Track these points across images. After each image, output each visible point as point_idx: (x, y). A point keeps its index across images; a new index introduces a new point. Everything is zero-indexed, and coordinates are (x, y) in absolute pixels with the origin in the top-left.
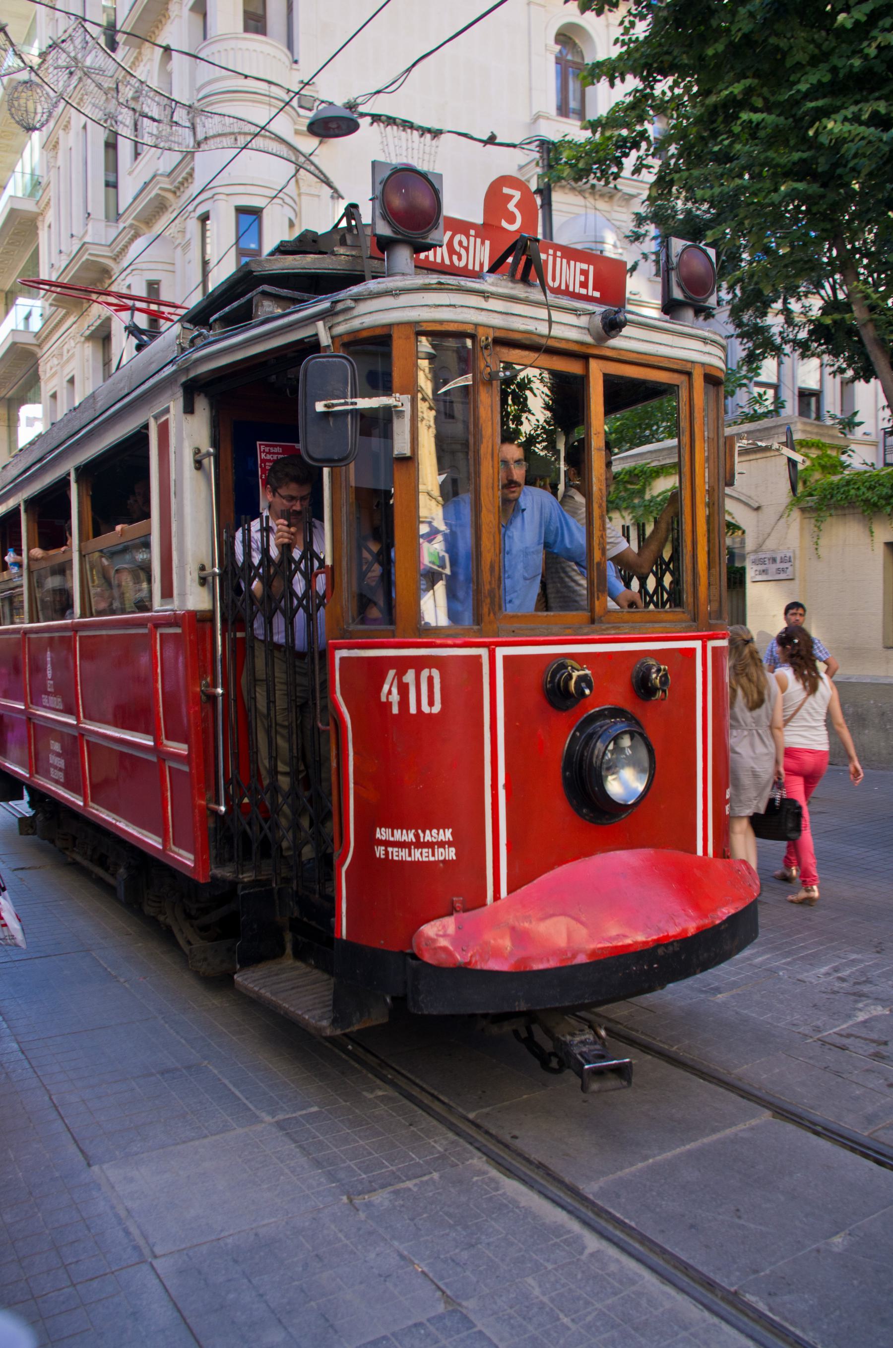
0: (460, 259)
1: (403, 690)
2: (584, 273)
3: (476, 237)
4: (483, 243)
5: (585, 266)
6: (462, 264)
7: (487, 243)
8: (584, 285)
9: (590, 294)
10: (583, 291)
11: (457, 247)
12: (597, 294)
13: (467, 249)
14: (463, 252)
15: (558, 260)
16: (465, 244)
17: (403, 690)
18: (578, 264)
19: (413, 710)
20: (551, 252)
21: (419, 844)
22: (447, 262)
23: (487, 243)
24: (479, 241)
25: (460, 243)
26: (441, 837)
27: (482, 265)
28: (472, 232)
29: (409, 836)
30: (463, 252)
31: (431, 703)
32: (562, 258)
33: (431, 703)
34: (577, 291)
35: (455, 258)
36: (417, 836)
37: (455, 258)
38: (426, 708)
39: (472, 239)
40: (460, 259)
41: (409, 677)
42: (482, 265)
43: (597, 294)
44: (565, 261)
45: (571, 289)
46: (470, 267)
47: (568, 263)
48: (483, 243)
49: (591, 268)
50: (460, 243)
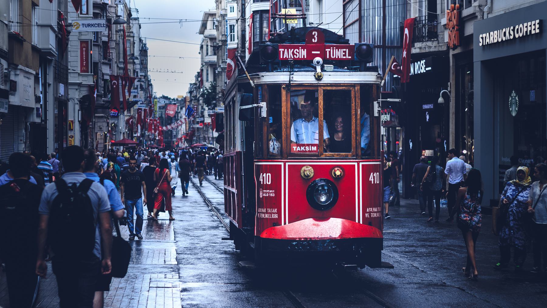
0: (297, 56)
1: (263, 178)
2: (345, 52)
3: (301, 49)
4: (304, 50)
5: (345, 50)
6: (297, 57)
7: (305, 50)
8: (345, 55)
9: (347, 58)
10: (345, 57)
11: (295, 53)
12: (350, 57)
13: (299, 53)
14: (297, 54)
15: (335, 50)
16: (298, 51)
17: (263, 178)
18: (342, 50)
19: (265, 183)
20: (332, 48)
21: (267, 213)
22: (292, 57)
23: (305, 50)
24: (302, 50)
25: (296, 52)
26: (274, 211)
27: (304, 56)
28: (300, 48)
29: (265, 210)
30: (297, 54)
31: (269, 182)
32: (336, 49)
33: (269, 182)
34: (342, 58)
35: (295, 56)
36: (266, 210)
37: (295, 56)
38: (268, 183)
39: (300, 50)
40: (297, 56)
41: (264, 175)
42: (304, 56)
43: (350, 57)
44: (337, 50)
45: (340, 57)
46: (300, 57)
47: (338, 50)
48: (304, 50)
49: (347, 50)
50: (296, 52)
